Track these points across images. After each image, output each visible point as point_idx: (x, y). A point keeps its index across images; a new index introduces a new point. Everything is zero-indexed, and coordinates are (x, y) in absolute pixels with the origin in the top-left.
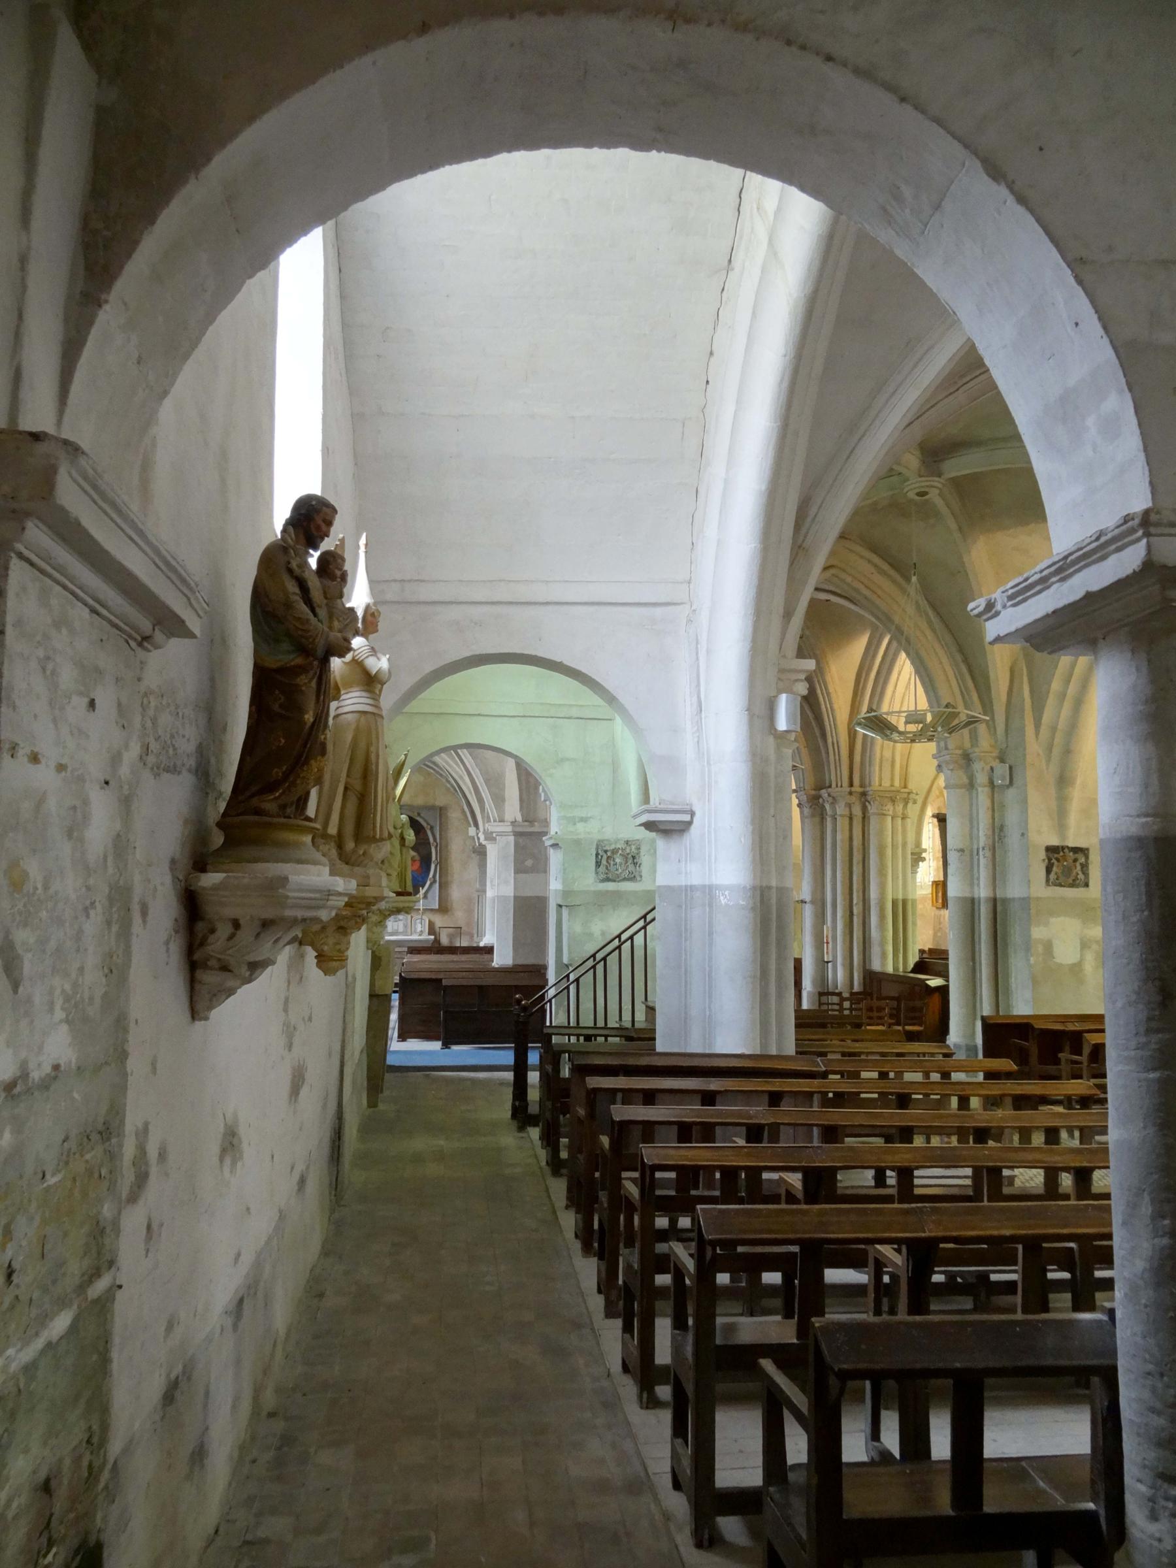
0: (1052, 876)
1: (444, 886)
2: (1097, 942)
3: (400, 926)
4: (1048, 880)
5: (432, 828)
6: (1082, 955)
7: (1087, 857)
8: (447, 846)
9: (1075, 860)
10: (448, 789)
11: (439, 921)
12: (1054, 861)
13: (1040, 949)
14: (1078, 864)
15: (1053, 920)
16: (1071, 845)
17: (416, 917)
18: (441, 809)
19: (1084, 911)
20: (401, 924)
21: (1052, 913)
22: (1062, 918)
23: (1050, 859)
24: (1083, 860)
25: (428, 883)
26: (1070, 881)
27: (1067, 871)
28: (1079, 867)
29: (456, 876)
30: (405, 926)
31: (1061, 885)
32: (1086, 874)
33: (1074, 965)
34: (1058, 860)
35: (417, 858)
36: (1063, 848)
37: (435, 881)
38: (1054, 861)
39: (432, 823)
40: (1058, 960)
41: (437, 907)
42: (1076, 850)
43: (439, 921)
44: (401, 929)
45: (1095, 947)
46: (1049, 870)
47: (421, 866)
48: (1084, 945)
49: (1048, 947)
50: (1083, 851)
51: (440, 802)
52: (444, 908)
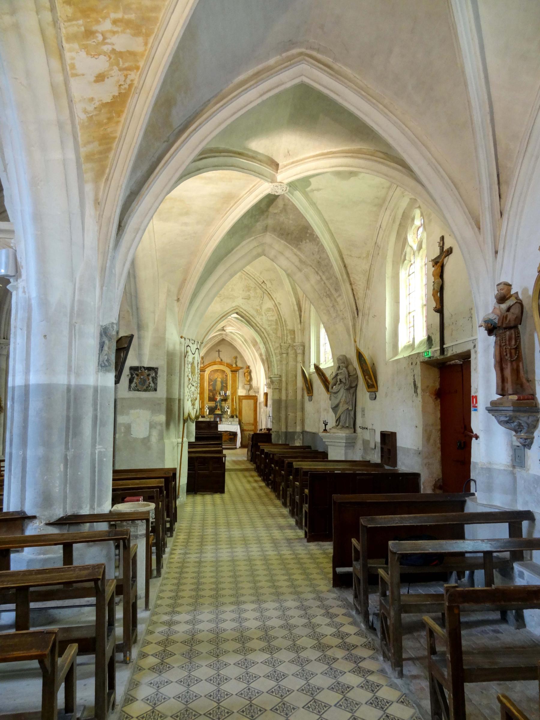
0: (133, 385)
2: (161, 424)
4: (130, 387)
6: (150, 432)
7: (156, 373)
9: (148, 375)
12: (134, 375)
13: (123, 429)
14: (150, 378)
15: (132, 411)
16: (146, 366)
19: (153, 406)
21: (131, 407)
22: (138, 410)
23: (132, 375)
24: (154, 375)
26: (145, 387)
27: (143, 382)
28: (151, 379)
31: (138, 390)
32: (156, 384)
33: (144, 438)
34: (137, 375)
36: (141, 367)
38: (134, 375)
40: (134, 436)
42: (149, 369)
45: (159, 427)
46: (131, 381)
48: (152, 426)
49: (128, 427)
50: (155, 370)
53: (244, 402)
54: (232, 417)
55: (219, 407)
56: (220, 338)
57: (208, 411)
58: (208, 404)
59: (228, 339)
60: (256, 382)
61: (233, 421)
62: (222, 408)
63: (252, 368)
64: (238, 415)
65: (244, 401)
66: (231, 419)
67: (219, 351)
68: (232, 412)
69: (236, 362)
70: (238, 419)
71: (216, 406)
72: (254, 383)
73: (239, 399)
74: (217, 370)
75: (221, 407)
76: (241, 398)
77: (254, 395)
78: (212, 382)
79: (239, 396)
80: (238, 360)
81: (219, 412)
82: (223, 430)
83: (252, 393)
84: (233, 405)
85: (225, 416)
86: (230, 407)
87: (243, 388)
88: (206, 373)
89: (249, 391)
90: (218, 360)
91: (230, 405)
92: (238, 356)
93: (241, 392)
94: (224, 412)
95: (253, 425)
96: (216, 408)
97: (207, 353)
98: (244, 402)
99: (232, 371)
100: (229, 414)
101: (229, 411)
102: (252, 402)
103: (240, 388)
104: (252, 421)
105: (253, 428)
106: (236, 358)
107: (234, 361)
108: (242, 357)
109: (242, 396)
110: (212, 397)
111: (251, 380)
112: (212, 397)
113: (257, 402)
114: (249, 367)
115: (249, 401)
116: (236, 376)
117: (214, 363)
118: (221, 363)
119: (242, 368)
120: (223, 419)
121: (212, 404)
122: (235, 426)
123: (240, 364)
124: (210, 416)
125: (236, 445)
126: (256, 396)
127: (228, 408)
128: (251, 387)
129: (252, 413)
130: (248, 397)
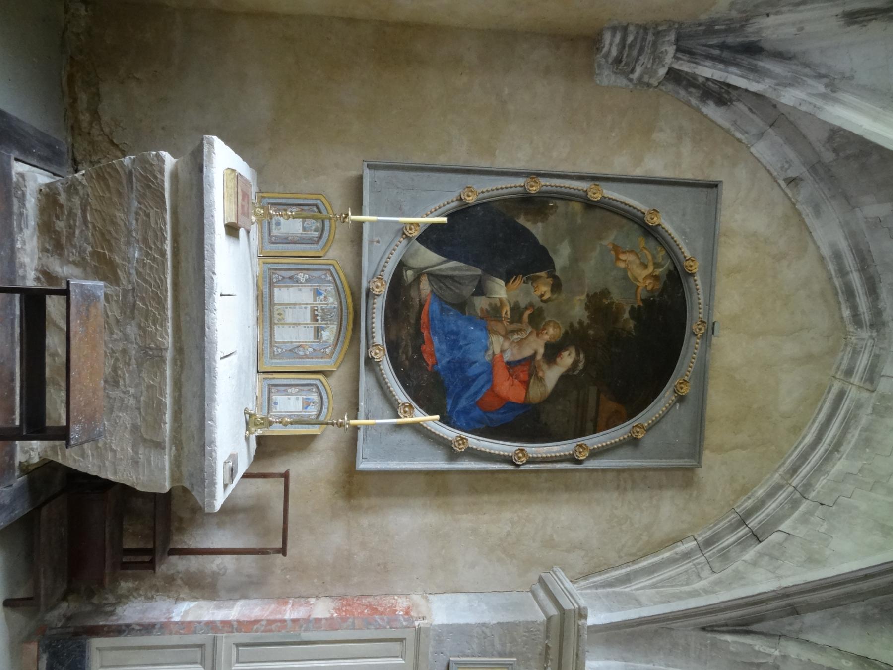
1: (435, 485)
3: (294, 333)
5: (633, 442)
8: (568, 488)
10: (745, 491)
11: (312, 469)
17: (335, 385)
18: (691, 469)
20: (305, 335)
25: (449, 433)
29: (466, 521)
30: (294, 351)
35: (536, 393)
37: (453, 454)
39: (649, 441)
41: (362, 466)
43: (312, 469)
44: (283, 335)
47: (509, 406)
51: (714, 470)
52: (355, 486)
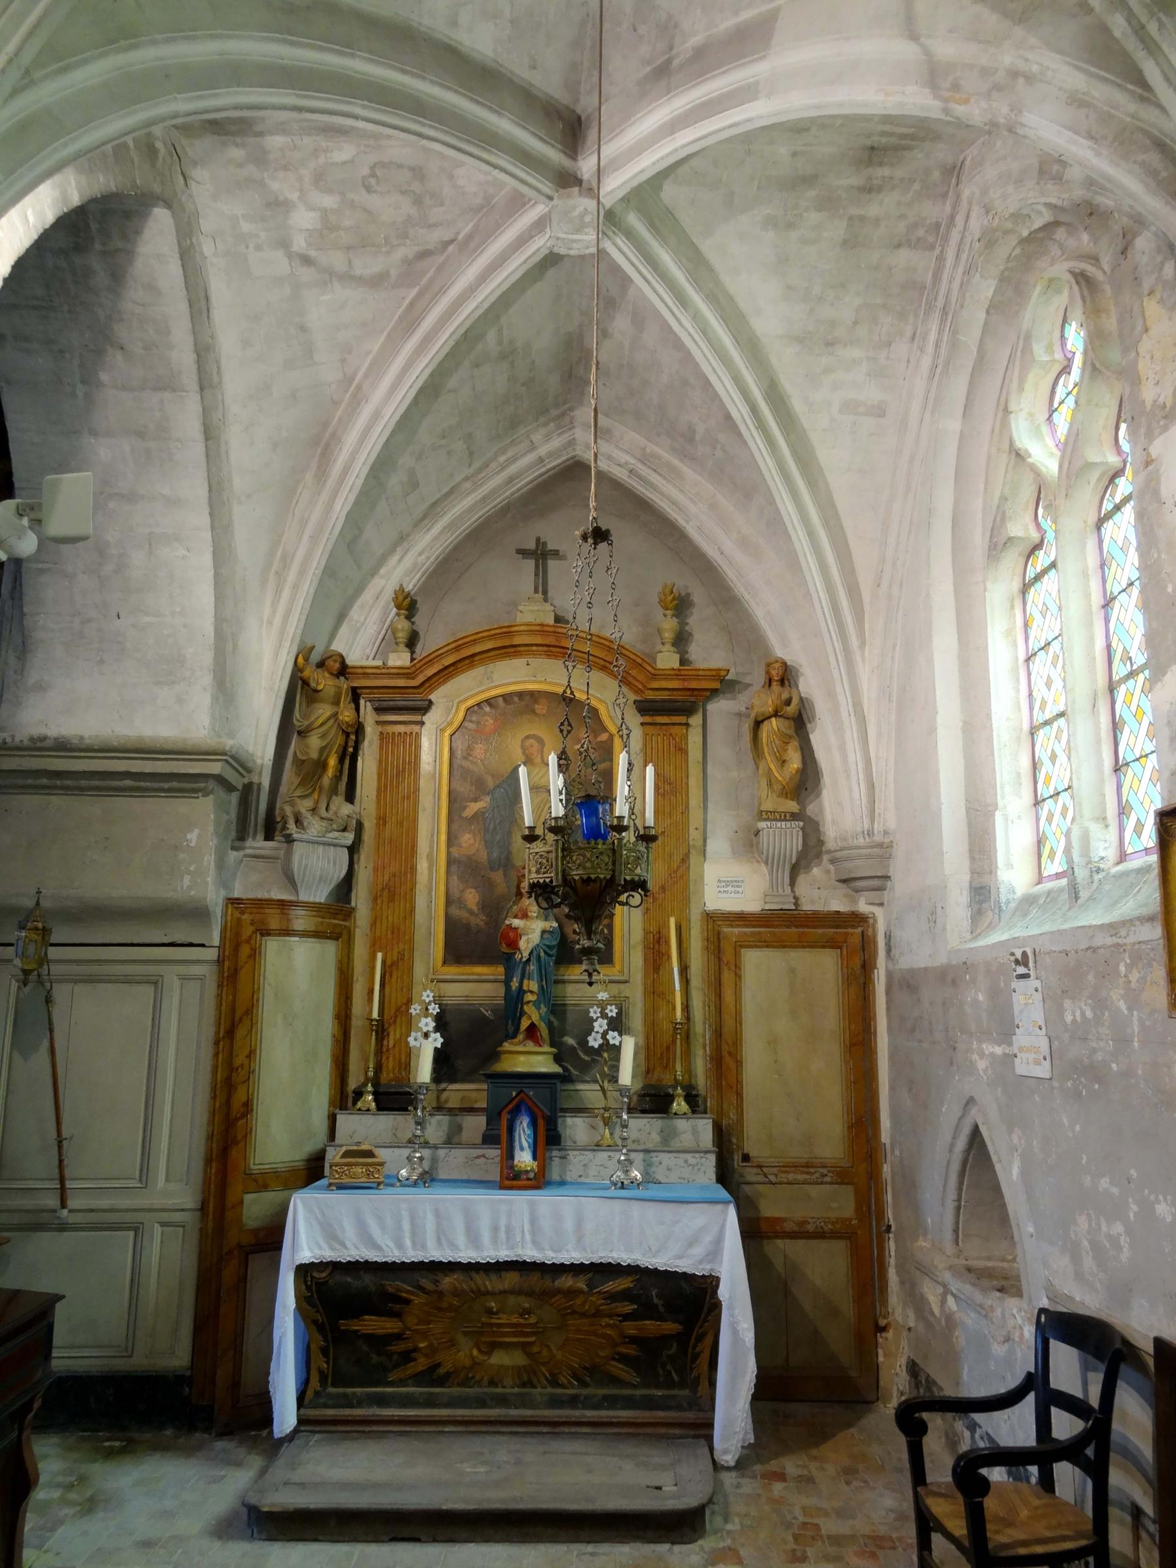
53: (760, 968)
54: (653, 1101)
55: (533, 1014)
56: (541, 450)
57: (437, 1040)
58: (439, 986)
59: (619, 454)
60: (860, 792)
61: (667, 1143)
62: (562, 1027)
63: (808, 685)
64: (701, 1080)
65: (754, 961)
66: (644, 1128)
67: (541, 555)
68: (655, 1056)
69: (681, 640)
70: (704, 1128)
71: (514, 1002)
72: (841, 809)
73: (715, 944)
74: (524, 702)
75: (557, 1010)
76: (728, 935)
77: (838, 904)
78: (484, 796)
79: (712, 918)
80: (695, 621)
81: (536, 1060)
82: (571, 1255)
83: (820, 894)
84: (656, 992)
85: (589, 1092)
86: (637, 1019)
87: (749, 844)
88: (432, 719)
89: (795, 871)
90: (534, 613)
91: (636, 994)
92: (694, 588)
93: (729, 882)
94: (581, 1060)
95: (842, 1177)
96: (506, 1020)
97: (448, 570)
98: (760, 968)
99: (646, 708)
100: (626, 1076)
101: (629, 1047)
102: (823, 967)
103: (718, 844)
104: (831, 1144)
105: (841, 1204)
106: (680, 605)
107: (669, 625)
108: (727, 600)
109: (741, 918)
110: (479, 921)
111: (806, 782)
112: (479, 921)
113: (867, 967)
114: (784, 676)
115: (801, 958)
116: (683, 751)
117: (506, 646)
118: (555, 642)
119: (722, 684)
120: (575, 1128)
121: (478, 986)
122: (696, 1218)
123: (709, 652)
124: (456, 1092)
125: (703, 1429)
126: (858, 919)
127: (617, 1024)
128: (813, 847)
129: (827, 1069)
130: (786, 927)
